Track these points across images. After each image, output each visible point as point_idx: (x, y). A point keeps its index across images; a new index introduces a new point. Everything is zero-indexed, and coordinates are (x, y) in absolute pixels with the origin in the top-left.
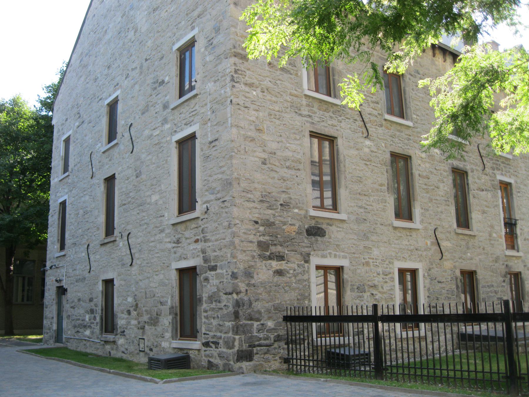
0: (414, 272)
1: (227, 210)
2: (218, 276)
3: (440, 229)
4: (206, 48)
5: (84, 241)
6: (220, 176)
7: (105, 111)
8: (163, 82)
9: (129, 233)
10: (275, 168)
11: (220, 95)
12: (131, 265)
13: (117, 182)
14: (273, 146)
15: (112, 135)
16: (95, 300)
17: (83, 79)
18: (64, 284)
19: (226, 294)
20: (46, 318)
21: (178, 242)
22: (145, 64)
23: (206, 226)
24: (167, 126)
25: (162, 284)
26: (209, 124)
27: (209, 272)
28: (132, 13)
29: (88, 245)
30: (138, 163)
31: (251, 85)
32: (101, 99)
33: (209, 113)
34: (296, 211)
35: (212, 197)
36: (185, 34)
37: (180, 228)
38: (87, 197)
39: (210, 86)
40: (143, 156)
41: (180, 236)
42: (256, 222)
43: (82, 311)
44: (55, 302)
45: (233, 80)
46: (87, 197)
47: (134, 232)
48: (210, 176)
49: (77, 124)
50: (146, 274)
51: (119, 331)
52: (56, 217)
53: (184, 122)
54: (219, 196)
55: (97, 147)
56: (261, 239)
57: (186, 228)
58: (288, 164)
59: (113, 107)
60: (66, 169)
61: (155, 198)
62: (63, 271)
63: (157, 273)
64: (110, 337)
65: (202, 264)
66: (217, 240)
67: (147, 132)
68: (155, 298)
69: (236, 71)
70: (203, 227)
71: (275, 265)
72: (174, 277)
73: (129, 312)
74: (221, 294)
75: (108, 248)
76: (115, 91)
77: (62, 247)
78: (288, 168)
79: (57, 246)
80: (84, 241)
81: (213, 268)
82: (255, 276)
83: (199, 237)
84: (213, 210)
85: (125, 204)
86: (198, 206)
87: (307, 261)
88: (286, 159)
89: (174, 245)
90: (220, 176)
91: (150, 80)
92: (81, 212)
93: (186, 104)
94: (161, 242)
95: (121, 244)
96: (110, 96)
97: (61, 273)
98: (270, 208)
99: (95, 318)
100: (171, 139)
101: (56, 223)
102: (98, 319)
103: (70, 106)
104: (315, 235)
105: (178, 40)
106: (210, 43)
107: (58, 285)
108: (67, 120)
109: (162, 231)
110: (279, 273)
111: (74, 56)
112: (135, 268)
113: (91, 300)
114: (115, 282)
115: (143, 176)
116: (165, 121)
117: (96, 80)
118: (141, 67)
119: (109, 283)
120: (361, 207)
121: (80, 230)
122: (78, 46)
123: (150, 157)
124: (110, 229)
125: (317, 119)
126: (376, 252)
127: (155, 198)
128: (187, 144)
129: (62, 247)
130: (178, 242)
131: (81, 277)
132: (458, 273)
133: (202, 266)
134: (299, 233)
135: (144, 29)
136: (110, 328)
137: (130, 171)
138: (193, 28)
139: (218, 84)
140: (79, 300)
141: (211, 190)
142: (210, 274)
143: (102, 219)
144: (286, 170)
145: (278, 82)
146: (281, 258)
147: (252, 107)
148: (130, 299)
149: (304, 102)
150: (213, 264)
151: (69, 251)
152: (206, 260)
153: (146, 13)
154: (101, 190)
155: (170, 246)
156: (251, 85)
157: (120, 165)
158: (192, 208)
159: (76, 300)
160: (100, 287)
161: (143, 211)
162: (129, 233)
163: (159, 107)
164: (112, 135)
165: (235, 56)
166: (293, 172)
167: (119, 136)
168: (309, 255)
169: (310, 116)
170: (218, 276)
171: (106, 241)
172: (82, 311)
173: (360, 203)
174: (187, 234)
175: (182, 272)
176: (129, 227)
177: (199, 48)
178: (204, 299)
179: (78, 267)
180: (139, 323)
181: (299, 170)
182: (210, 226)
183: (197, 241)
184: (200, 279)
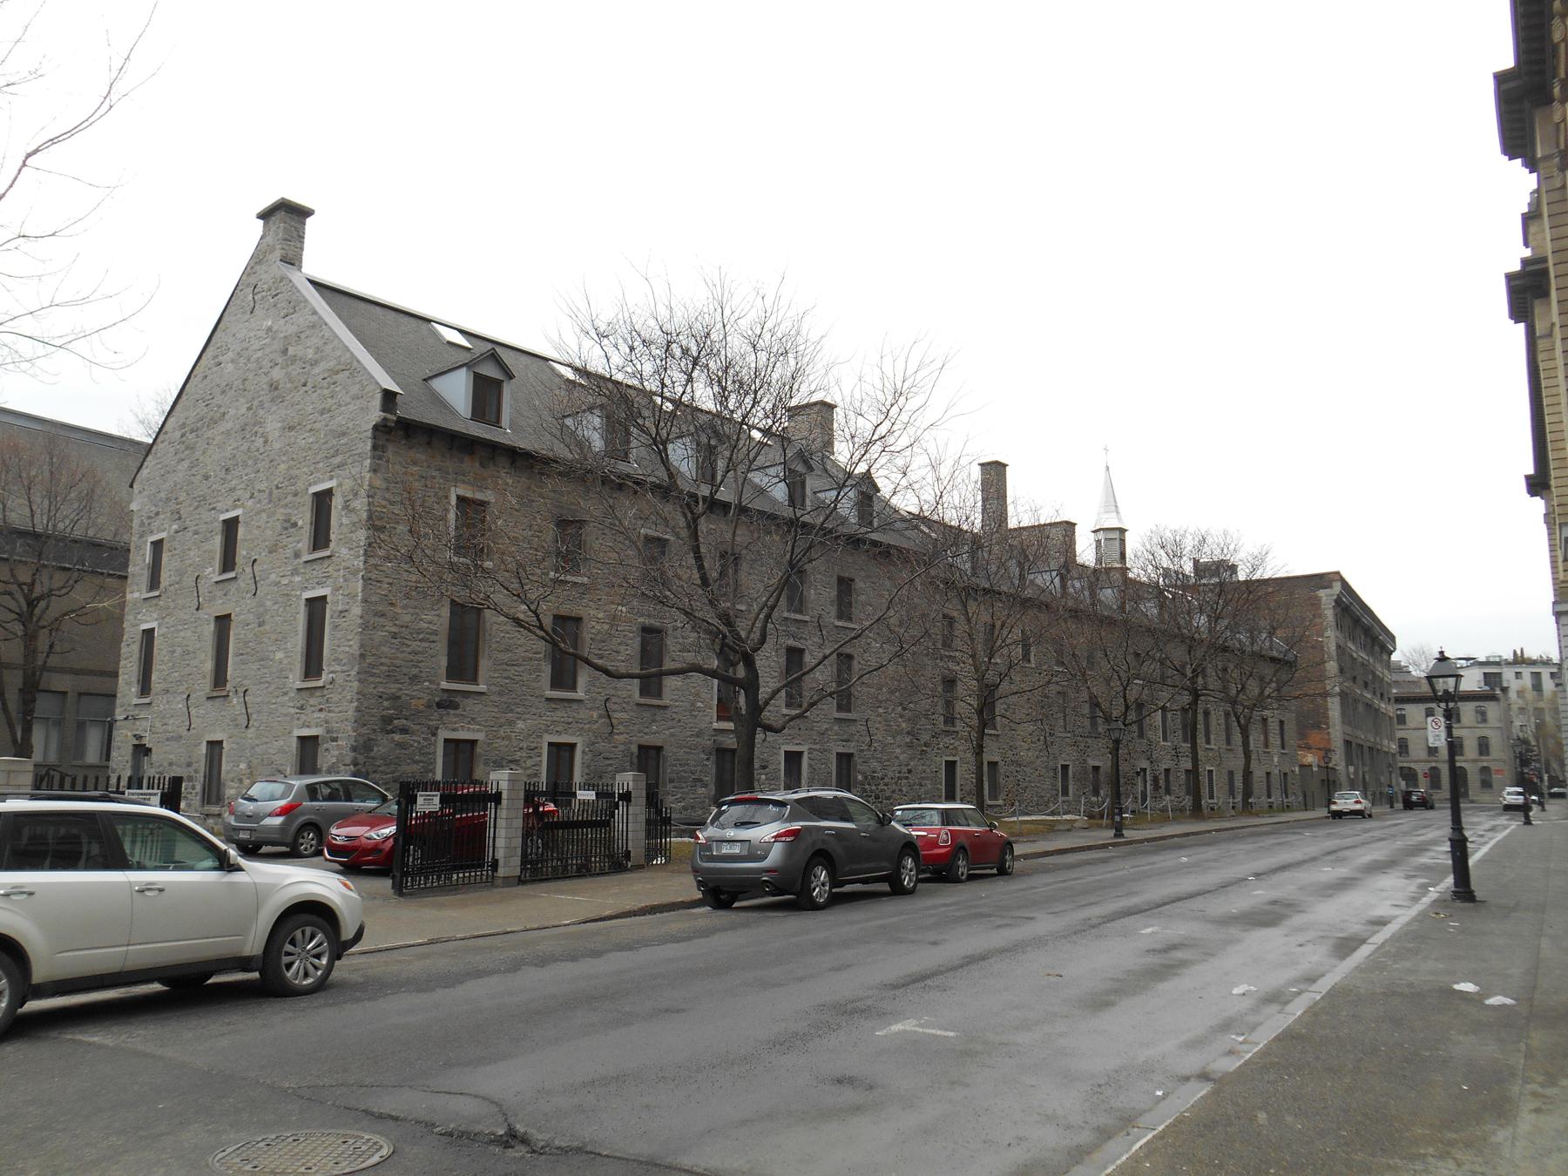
3: (614, 699)
5: (182, 689)
7: (219, 527)
8: (295, 525)
13: (233, 625)
14: (407, 618)
15: (228, 563)
17: (186, 464)
18: (146, 742)
24: (297, 579)
25: (281, 751)
28: (261, 412)
35: (338, 668)
37: (304, 693)
38: (189, 633)
40: (268, 603)
46: (189, 633)
47: (252, 689)
49: (175, 527)
52: (135, 648)
57: (312, 695)
59: (231, 526)
60: (154, 583)
61: (279, 655)
62: (146, 724)
64: (215, 809)
71: (397, 737)
73: (241, 781)
75: (218, 702)
76: (235, 507)
77: (145, 687)
80: (182, 689)
81: (335, 739)
87: (434, 735)
91: (281, 513)
92: (179, 650)
97: (142, 727)
98: (397, 681)
101: (136, 656)
102: (199, 788)
103: (163, 495)
104: (448, 707)
105: (315, 483)
108: (157, 514)
109: (285, 694)
110: (400, 745)
111: (171, 420)
112: (251, 730)
113: (189, 765)
115: (267, 627)
116: (295, 572)
117: (207, 478)
118: (271, 493)
119: (215, 746)
122: (178, 408)
124: (220, 678)
126: (520, 725)
127: (279, 655)
128: (316, 607)
129: (145, 687)
130: (302, 708)
132: (634, 749)
134: (429, 707)
135: (277, 446)
136: (214, 799)
137: (251, 616)
138: (331, 478)
140: (171, 764)
143: (209, 666)
146: (404, 731)
148: (243, 766)
151: (159, 702)
154: (209, 629)
155: (293, 711)
157: (239, 606)
158: (319, 674)
160: (203, 749)
163: (289, 552)
164: (228, 563)
166: (426, 645)
167: (238, 569)
174: (312, 701)
175: (302, 739)
182: (335, 697)
184: (321, 750)
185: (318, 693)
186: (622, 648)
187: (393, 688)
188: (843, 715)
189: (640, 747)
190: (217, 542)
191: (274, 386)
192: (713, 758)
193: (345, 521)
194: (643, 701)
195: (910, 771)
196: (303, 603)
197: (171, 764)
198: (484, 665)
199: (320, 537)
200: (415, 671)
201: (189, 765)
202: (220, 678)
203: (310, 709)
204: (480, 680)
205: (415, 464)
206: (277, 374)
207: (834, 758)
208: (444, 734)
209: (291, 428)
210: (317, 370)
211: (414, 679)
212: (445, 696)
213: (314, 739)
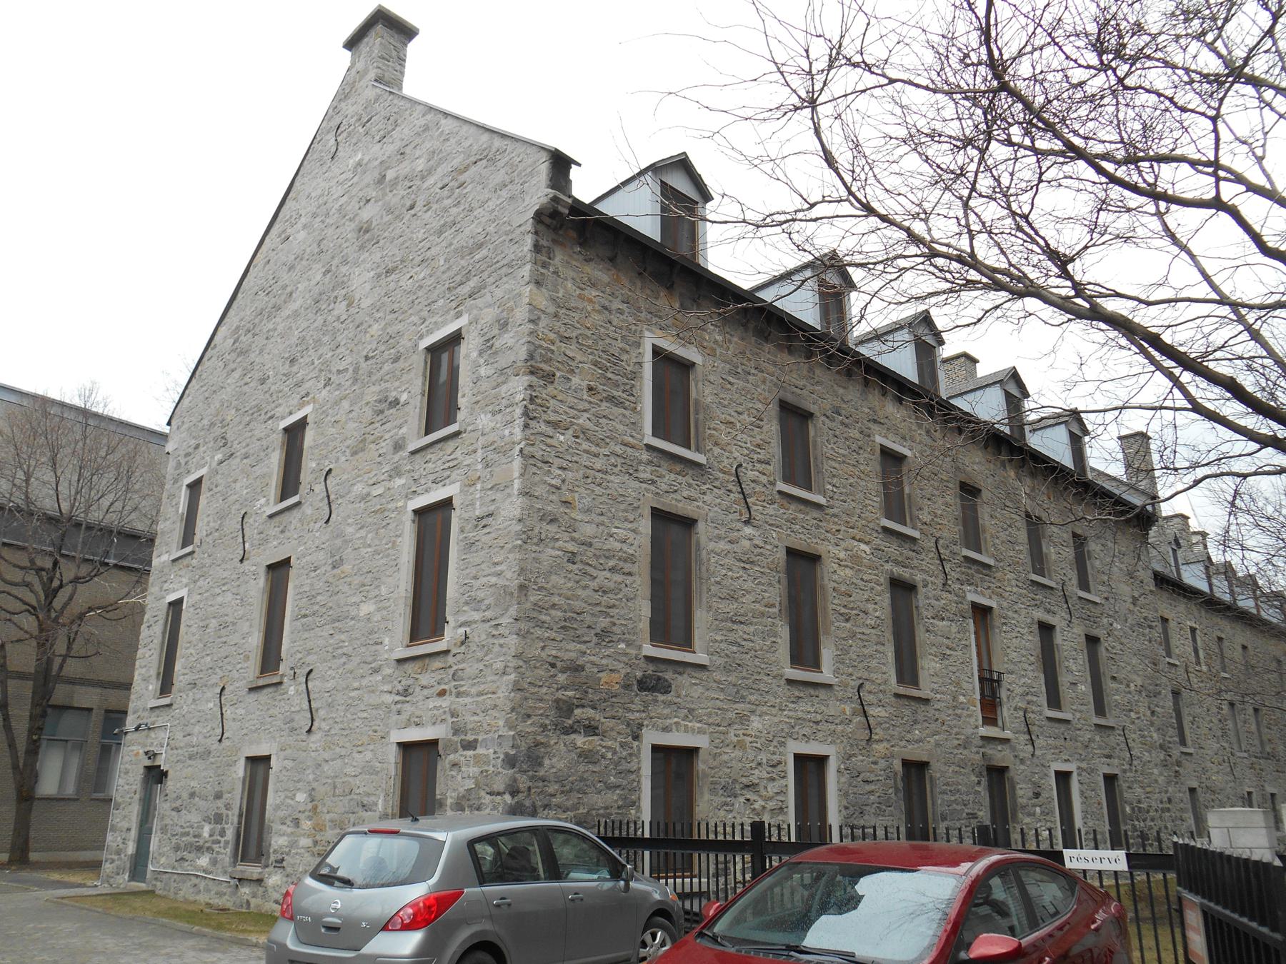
0: (821, 760)
1: (502, 641)
2: (478, 760)
3: (868, 686)
4: (481, 354)
5: (214, 679)
6: (493, 580)
7: (278, 439)
8: (396, 402)
9: (311, 671)
10: (590, 570)
11: (502, 438)
12: (309, 731)
13: (292, 573)
14: (588, 530)
15: (289, 484)
16: (226, 796)
17: (236, 375)
18: (161, 762)
19: (491, 794)
20: (114, 829)
21: (406, 692)
22: (364, 365)
23: (461, 666)
24: (399, 482)
25: (369, 770)
26: (479, 486)
27: (461, 752)
28: (344, 269)
29: (223, 689)
30: (338, 542)
31: (555, 425)
32: (271, 417)
33: (480, 466)
34: (622, 646)
35: (477, 616)
36: (444, 324)
37: (409, 667)
38: (229, 596)
39: (484, 421)
40: (350, 530)
41: (410, 682)
42: (553, 665)
43: (194, 818)
44: (137, 796)
45: (526, 413)
46: (229, 596)
47: (320, 668)
48: (476, 578)
49: (219, 457)
50: (338, 750)
51: (272, 858)
52: (158, 629)
53: (432, 477)
54: (488, 614)
55: (258, 504)
56: (559, 695)
57: (424, 669)
58: (611, 563)
59: (295, 433)
60: (187, 538)
61: (366, 608)
62: (163, 736)
63: (360, 749)
64: (253, 871)
65: (450, 736)
66: (480, 694)
67: (359, 488)
68: (352, 796)
69: (532, 399)
70: (455, 668)
71: (580, 740)
72: (392, 756)
73: (297, 822)
74: (483, 793)
75: (264, 696)
76: (302, 406)
77: (166, 686)
78: (612, 570)
79: (154, 686)
80: (214, 679)
81: (470, 745)
82: (547, 762)
83: (446, 687)
84: (477, 639)
85: (305, 616)
86: (448, 631)
87: (636, 737)
88: (609, 555)
89: (398, 698)
90: (493, 580)
91: (372, 394)
92: (214, 623)
93: (439, 446)
94: (373, 692)
95: (292, 691)
96: (291, 413)
97: (157, 741)
98: (578, 639)
99: (222, 833)
100: (405, 506)
101: (157, 641)
102: (230, 834)
103: (206, 422)
104: (653, 689)
105: (430, 332)
106: (488, 346)
107: (148, 763)
108: (197, 447)
109: (376, 671)
110: (587, 756)
111: (222, 329)
112: (315, 737)
113: (218, 796)
114: (273, 762)
115: (347, 567)
116: (396, 472)
117: (263, 381)
118: (356, 370)
119: (259, 763)
120: (733, 643)
121: (208, 659)
122: (231, 312)
123: (362, 533)
124: (270, 657)
125: (664, 487)
126: (756, 724)
127: (366, 608)
128: (433, 518)
129: (166, 686)
130: (406, 692)
131: (201, 749)
132: (897, 765)
133: (450, 740)
134: (627, 687)
135: (366, 303)
136: (252, 851)
137: (321, 556)
139: (499, 417)
140: (192, 795)
141: (475, 603)
142: (461, 756)
143: (255, 640)
144: (608, 575)
145: (603, 421)
146: (591, 729)
147: (557, 462)
148: (301, 797)
149: (645, 456)
150: (470, 737)
151: (181, 697)
152: (456, 732)
153: (372, 273)
154: (257, 586)
155: (389, 699)
156: (555, 425)
157: (301, 541)
158: (437, 631)
159: (185, 796)
160: (240, 770)
161: (341, 631)
162: (311, 671)
163: (386, 446)
164: (289, 484)
165: (532, 373)
166: (618, 578)
167: (304, 489)
168: (640, 726)
169: (653, 482)
170: (478, 760)
171: (261, 682)
172: (194, 818)
173: (732, 637)
174: (425, 679)
175: (406, 748)
176: (310, 659)
177: (468, 352)
178: (449, 801)
179: (197, 729)
180: (316, 843)
181: (630, 574)
182: (471, 668)
183: (442, 693)
184: (443, 765)
185: (437, 664)
186: (870, 607)
187: (571, 651)
188: (1102, 722)
189: (906, 763)
190: (275, 460)
191: (364, 229)
192: (984, 781)
193: (483, 371)
194: (902, 690)
195: (1170, 800)
196: (409, 516)
197: (192, 795)
198: (701, 618)
199: (440, 405)
200: (603, 622)
201: (218, 796)
202: (270, 657)
203: (418, 694)
204: (697, 643)
205: (593, 285)
206: (367, 213)
207: (1101, 779)
208: (652, 737)
209: (389, 272)
210: (431, 180)
211: (604, 635)
212: (651, 669)
213: (431, 746)
